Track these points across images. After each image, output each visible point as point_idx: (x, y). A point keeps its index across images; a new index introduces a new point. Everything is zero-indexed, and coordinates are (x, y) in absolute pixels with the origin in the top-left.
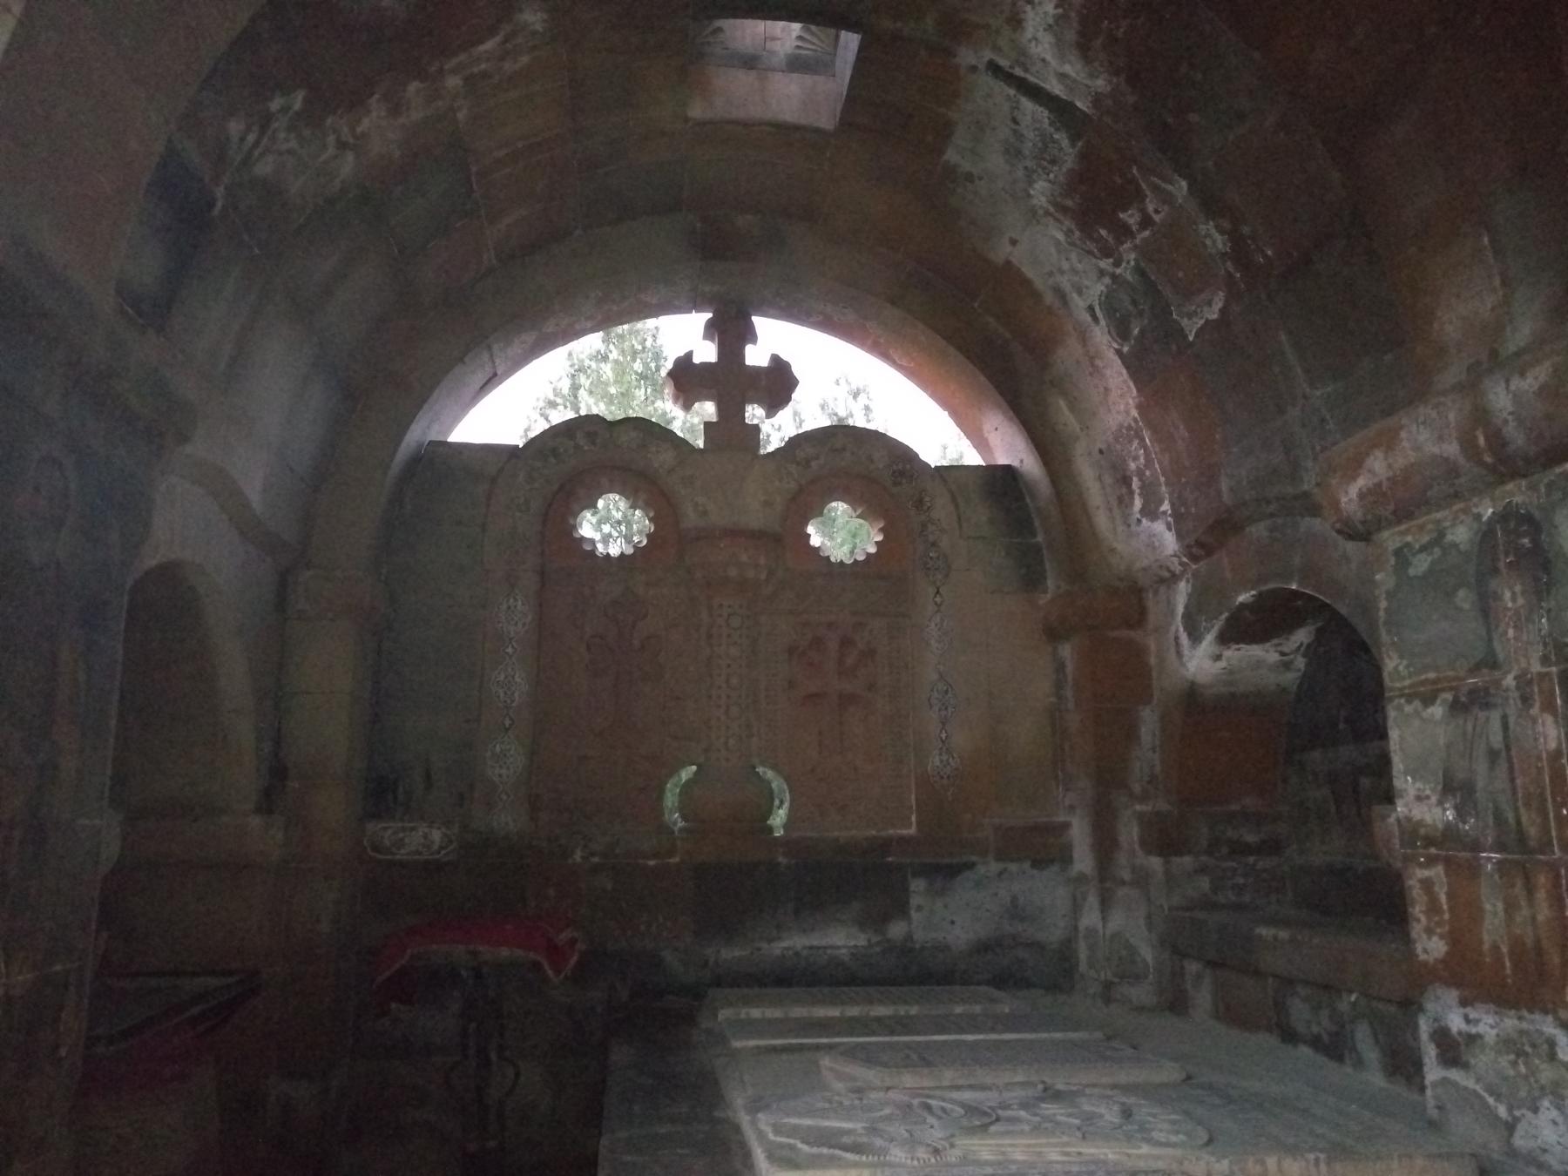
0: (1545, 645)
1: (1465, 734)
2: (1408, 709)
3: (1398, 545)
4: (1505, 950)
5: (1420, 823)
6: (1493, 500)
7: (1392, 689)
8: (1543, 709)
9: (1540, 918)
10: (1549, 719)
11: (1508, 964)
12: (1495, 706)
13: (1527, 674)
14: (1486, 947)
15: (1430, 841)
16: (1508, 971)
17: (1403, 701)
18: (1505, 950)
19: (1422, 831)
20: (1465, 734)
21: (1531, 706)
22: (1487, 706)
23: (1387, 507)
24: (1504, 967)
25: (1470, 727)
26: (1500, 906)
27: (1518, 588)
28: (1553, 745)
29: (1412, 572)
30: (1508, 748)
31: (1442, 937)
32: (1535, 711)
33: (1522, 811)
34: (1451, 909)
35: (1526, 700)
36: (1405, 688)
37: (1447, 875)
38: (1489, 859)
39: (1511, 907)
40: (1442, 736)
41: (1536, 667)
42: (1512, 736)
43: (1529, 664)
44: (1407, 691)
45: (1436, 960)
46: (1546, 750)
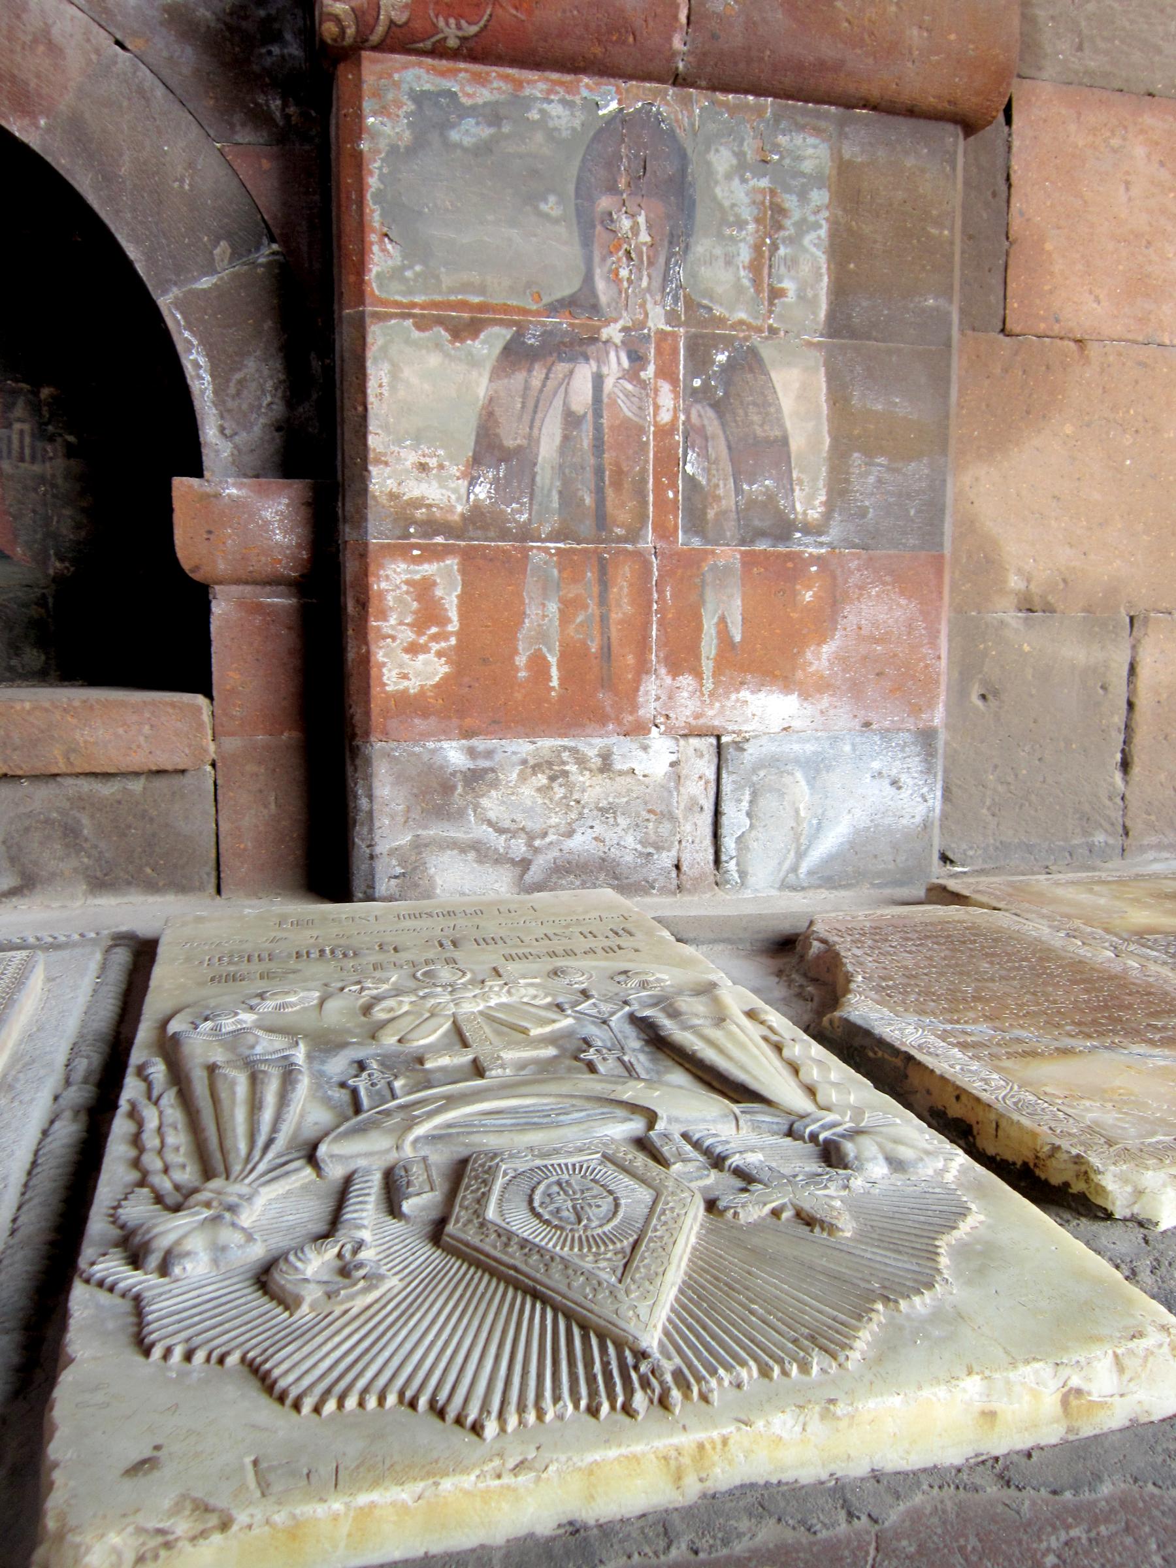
0: (676, 299)
1: (527, 387)
2: (416, 334)
3: (427, 87)
4: (553, 660)
5: (417, 503)
6: (618, 91)
7: (385, 303)
8: (661, 373)
9: (615, 616)
10: (665, 387)
11: (554, 672)
12: (587, 359)
13: (643, 329)
14: (521, 660)
15: (432, 527)
16: (555, 683)
17: (409, 322)
18: (553, 660)
19: (420, 513)
20: (527, 387)
21: (644, 369)
22: (572, 359)
23: (463, 22)
24: (549, 678)
25: (536, 383)
26: (553, 608)
27: (641, 219)
28: (665, 417)
29: (454, 136)
30: (598, 414)
31: (439, 654)
32: (649, 372)
33: (610, 492)
34: (462, 617)
35: (637, 359)
36: (413, 305)
37: (463, 571)
38: (546, 550)
39: (569, 608)
40: (481, 386)
41: (657, 321)
42: (605, 400)
43: (646, 315)
44: (416, 311)
45: (422, 690)
46: (655, 422)
